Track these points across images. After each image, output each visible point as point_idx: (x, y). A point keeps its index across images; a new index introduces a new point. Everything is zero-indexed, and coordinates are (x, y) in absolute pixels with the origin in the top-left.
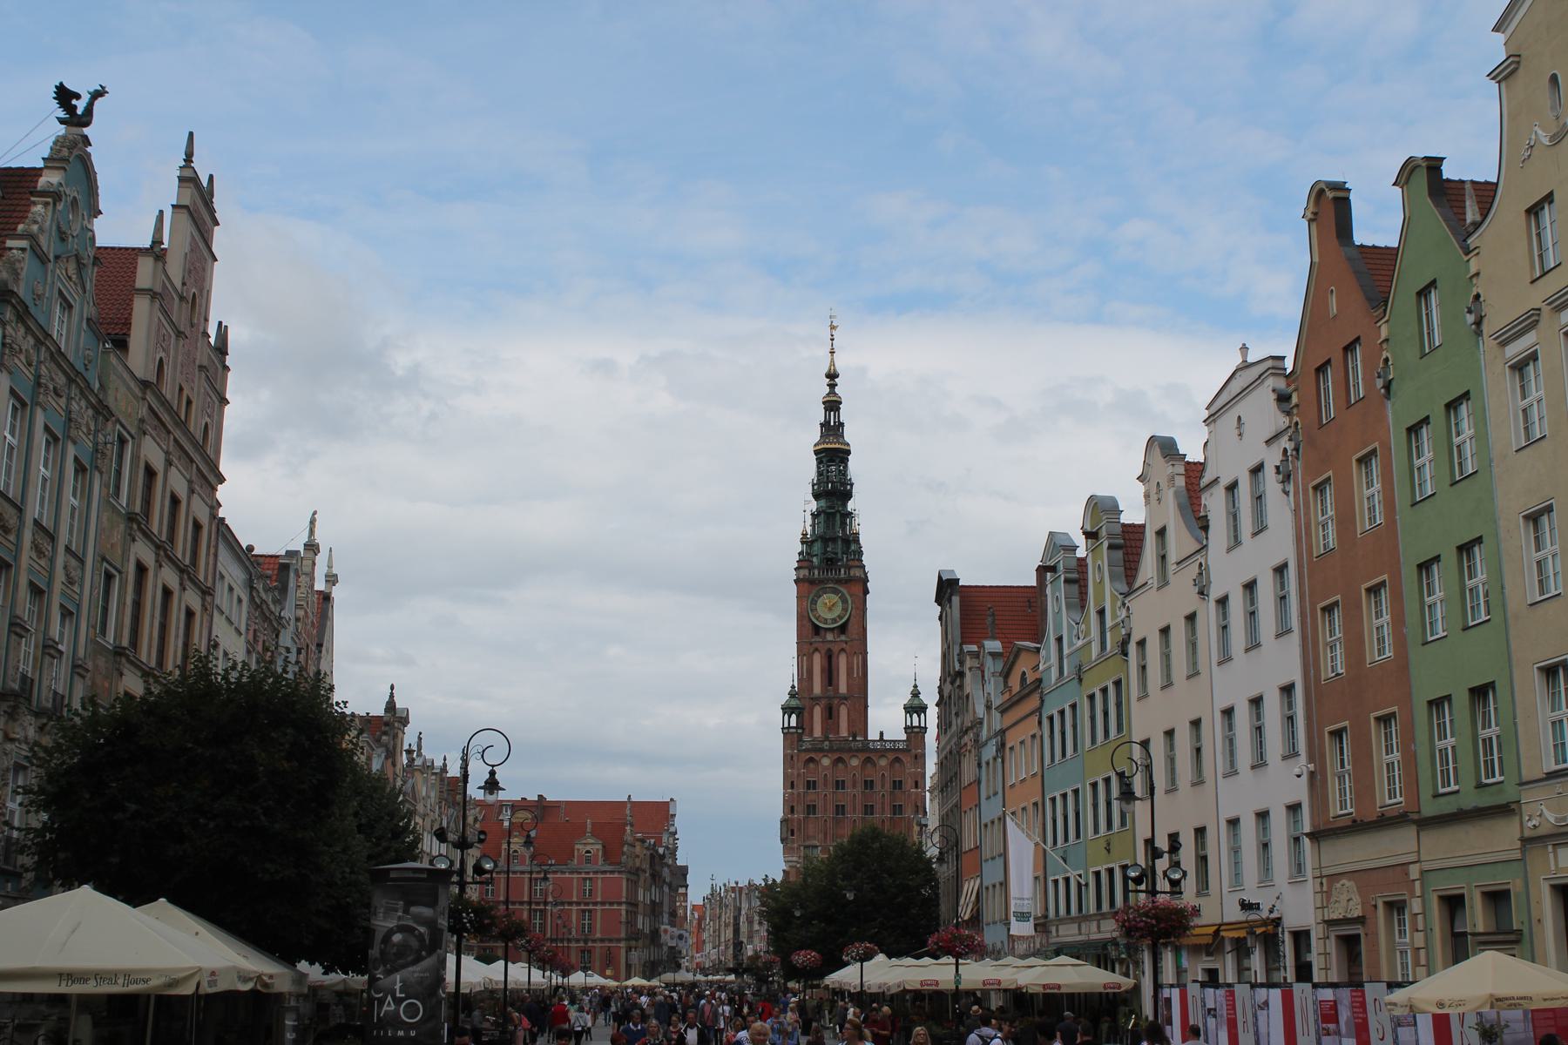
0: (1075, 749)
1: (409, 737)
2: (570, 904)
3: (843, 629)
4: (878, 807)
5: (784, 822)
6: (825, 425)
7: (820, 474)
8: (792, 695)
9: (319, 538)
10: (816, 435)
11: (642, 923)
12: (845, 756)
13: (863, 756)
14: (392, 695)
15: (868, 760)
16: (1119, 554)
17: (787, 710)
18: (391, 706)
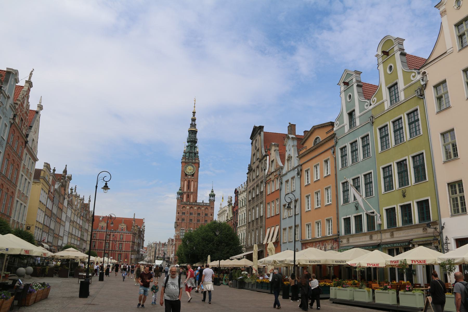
1: (72, 185)
3: (193, 175)
4: (201, 220)
6: (191, 124)
7: (189, 136)
8: (180, 190)
9: (32, 80)
10: (189, 126)
11: (136, 248)
13: (197, 207)
14: (66, 168)
15: (199, 208)
18: (65, 171)
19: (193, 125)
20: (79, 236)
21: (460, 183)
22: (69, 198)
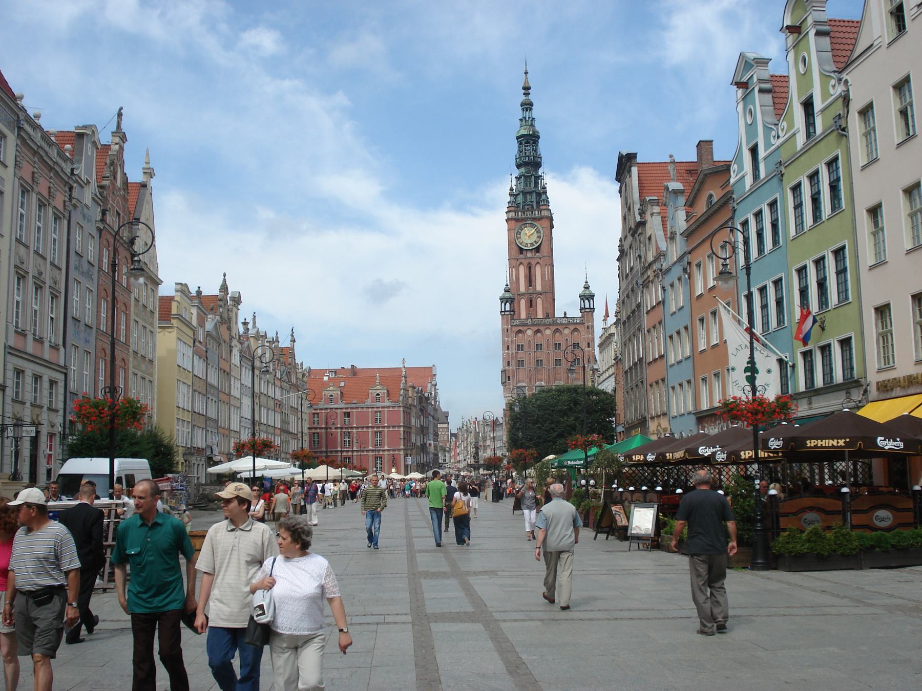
0: (775, 242)
1: (244, 313)
2: (368, 427)
3: (538, 249)
5: (503, 371)
8: (506, 291)
12: (542, 328)
15: (557, 330)
16: (826, 41)
17: (503, 300)
18: (224, 288)
19: (527, 121)
20: (278, 425)
21: (887, 306)
22: (241, 343)
